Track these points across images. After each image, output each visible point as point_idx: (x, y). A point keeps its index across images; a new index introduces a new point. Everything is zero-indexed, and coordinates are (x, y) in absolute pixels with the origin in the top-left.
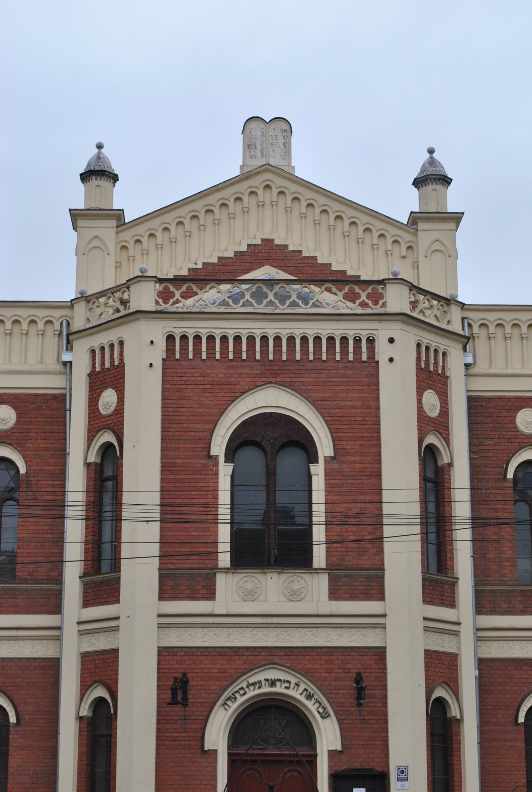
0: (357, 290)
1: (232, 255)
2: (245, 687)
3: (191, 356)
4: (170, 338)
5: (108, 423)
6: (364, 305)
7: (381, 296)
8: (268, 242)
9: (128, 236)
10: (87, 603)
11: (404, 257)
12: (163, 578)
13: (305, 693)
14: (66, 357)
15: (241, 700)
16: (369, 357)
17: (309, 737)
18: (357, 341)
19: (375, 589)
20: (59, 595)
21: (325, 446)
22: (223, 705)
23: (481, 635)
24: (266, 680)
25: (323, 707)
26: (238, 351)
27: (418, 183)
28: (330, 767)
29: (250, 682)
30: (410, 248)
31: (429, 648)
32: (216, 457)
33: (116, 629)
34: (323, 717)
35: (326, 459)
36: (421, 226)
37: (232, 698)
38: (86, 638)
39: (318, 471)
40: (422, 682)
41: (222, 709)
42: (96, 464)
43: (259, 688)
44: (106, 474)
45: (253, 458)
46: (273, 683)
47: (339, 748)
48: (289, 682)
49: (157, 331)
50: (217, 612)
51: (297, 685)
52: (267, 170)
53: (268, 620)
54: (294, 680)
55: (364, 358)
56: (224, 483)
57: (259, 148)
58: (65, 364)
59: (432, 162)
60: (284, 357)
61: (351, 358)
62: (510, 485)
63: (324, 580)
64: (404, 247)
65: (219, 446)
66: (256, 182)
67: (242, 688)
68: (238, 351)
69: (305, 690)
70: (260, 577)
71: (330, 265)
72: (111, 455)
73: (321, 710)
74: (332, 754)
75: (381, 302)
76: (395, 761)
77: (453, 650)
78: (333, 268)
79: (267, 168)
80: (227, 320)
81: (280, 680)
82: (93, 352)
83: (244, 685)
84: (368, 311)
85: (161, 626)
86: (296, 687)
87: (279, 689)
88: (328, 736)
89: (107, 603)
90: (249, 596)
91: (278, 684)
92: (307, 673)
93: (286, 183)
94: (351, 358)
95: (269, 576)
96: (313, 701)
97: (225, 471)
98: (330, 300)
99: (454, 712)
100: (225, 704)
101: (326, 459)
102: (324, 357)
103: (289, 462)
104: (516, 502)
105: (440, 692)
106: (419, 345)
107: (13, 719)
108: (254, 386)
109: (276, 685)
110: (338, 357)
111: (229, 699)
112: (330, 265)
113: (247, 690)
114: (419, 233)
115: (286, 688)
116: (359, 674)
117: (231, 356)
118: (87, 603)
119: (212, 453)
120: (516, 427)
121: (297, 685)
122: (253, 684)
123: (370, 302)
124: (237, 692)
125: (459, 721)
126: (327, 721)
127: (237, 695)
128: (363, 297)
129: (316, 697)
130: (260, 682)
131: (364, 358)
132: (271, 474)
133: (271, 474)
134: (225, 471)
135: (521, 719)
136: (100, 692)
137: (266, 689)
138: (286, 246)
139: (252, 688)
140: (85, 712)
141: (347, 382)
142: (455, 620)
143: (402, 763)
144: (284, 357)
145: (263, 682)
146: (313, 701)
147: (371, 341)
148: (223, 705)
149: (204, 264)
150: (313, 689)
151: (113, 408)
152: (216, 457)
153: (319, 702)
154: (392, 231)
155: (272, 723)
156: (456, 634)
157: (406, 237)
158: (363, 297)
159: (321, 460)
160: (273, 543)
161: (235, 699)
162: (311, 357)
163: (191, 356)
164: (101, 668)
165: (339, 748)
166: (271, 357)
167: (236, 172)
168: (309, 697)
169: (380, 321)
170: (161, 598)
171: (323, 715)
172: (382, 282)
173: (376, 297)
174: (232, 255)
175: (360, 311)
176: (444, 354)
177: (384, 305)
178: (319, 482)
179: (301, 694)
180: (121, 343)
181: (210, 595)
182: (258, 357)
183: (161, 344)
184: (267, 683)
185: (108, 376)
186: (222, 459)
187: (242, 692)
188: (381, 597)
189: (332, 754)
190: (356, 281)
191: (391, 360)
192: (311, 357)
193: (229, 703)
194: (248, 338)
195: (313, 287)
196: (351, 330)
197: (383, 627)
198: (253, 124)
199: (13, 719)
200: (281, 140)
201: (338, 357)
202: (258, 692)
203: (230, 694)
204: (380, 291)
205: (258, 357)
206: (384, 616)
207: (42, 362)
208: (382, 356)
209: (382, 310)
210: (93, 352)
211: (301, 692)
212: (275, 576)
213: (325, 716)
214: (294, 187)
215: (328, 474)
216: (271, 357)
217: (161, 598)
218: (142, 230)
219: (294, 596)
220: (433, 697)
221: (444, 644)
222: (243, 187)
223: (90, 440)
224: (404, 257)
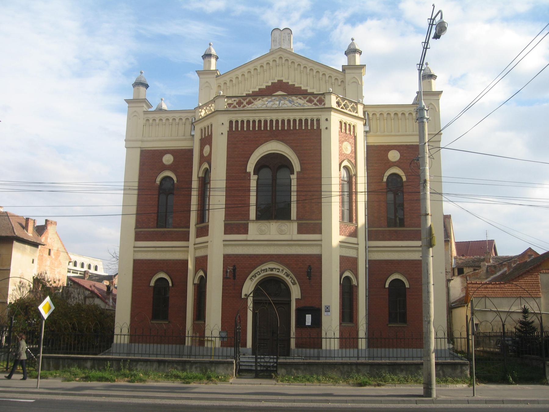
0: (313, 98)
1: (265, 87)
3: (239, 129)
4: (231, 122)
5: (206, 159)
6: (315, 104)
7: (323, 101)
8: (280, 81)
9: (221, 81)
10: (198, 236)
11: (340, 86)
12: (226, 226)
14: (192, 133)
15: (258, 277)
16: (317, 127)
17: (256, 292)
18: (312, 121)
19: (317, 228)
20: (188, 233)
21: (297, 167)
23: (368, 249)
26: (260, 126)
27: (346, 53)
28: (296, 306)
30: (342, 81)
31: (342, 255)
32: (250, 173)
33: (207, 247)
34: (293, 284)
35: (298, 173)
36: (347, 71)
37: (255, 276)
38: (197, 251)
39: (294, 177)
40: (338, 269)
41: (250, 281)
42: (202, 177)
44: (205, 182)
45: (267, 173)
46: (272, 270)
47: (300, 298)
49: (225, 119)
50: (248, 239)
51: (283, 270)
52: (281, 51)
53: (271, 242)
54: (281, 269)
55: (315, 128)
56: (253, 184)
57: (278, 41)
58: (191, 135)
59: (352, 44)
60: (280, 129)
61: (309, 128)
62: (385, 184)
63: (295, 226)
64: (340, 81)
65: (250, 168)
66: (276, 56)
68: (260, 126)
70: (268, 224)
71: (307, 90)
72: (207, 172)
74: (297, 300)
75: (323, 103)
76: (324, 303)
77: (355, 256)
78: (302, 89)
79: (281, 49)
80: (255, 113)
82: (202, 130)
83: (260, 270)
84: (317, 107)
85: (224, 245)
87: (274, 272)
88: (296, 292)
89: (205, 236)
90: (262, 233)
91: (274, 270)
92: (288, 266)
93: (289, 56)
94: (309, 128)
95: (271, 223)
97: (254, 179)
98: (300, 102)
99: (354, 282)
100: (251, 278)
101: (298, 173)
102: (297, 128)
103: (282, 174)
104: (387, 192)
105: (347, 274)
106: (341, 122)
107: (170, 285)
108: (266, 141)
110: (303, 128)
111: (253, 276)
112: (294, 85)
114: (346, 75)
116: (310, 266)
117: (257, 129)
118: (198, 236)
119: (248, 171)
120: (388, 158)
121: (283, 270)
123: (318, 104)
125: (357, 287)
126: (295, 286)
128: (315, 101)
130: (266, 269)
131: (315, 128)
132: (274, 179)
133: (274, 179)
134: (254, 179)
135: (387, 286)
136: (201, 273)
138: (288, 83)
140: (196, 282)
141: (308, 139)
142: (356, 242)
143: (328, 304)
144: (280, 129)
147: (318, 121)
149: (253, 92)
150: (289, 272)
151: (208, 153)
152: (250, 173)
154: (334, 75)
155: (272, 287)
156: (357, 249)
157: (340, 77)
158: (315, 101)
159: (295, 173)
160: (274, 209)
162: (292, 128)
163: (239, 129)
164: (202, 263)
165: (300, 298)
166: (274, 129)
167: (268, 52)
168: (288, 276)
169: (322, 111)
170: (225, 233)
172: (323, 94)
173: (321, 101)
174: (265, 87)
175: (314, 107)
176: (354, 126)
177: (324, 105)
178: (294, 182)
180: (212, 125)
181: (246, 232)
182: (268, 129)
183: (227, 125)
185: (206, 140)
186: (252, 173)
188: (320, 232)
189: (297, 300)
190: (312, 94)
191: (326, 128)
192: (292, 128)
193: (253, 278)
194: (264, 121)
195: (294, 98)
196: (309, 115)
197: (321, 245)
198: (275, 32)
199: (170, 285)
200: (287, 38)
201: (303, 128)
202: (265, 273)
204: (323, 98)
205: (268, 129)
206: (321, 240)
207: (184, 136)
208: (323, 127)
209: (323, 107)
210: (202, 130)
212: (274, 224)
213: (294, 284)
214: (292, 57)
215: (298, 179)
216: (274, 129)
217: (225, 233)
218: (227, 79)
219: (281, 232)
220: (344, 276)
221: (351, 253)
222: (270, 58)
223: (200, 167)
224: (340, 86)
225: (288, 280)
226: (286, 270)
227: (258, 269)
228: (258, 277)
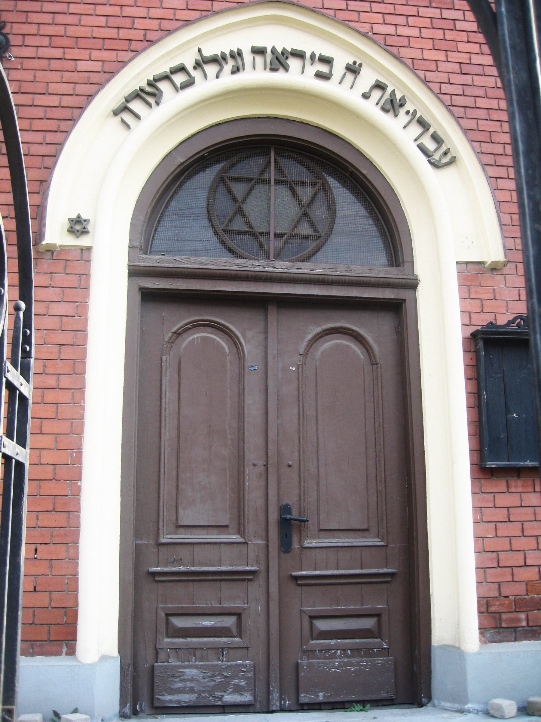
2: (190, 67)
13: (376, 94)
22: (116, 113)
24: (259, 51)
25: (435, 138)
29: (207, 53)
34: (435, 165)
37: (149, 93)
43: (236, 70)
48: (327, 61)
51: (353, 70)
54: (341, 60)
67: (182, 69)
69: (379, 86)
73: (431, 146)
81: (299, 55)
86: (350, 77)
87: (297, 76)
91: (294, 63)
96: (403, 118)
100: (125, 109)
109: (286, 69)
111: (138, 95)
113: (197, 75)
115: (319, 75)
121: (353, 70)
122: (214, 60)
124: (166, 77)
127: (163, 86)
129: (409, 106)
130: (237, 55)
137: (256, 75)
139: (211, 69)
145: (248, 57)
146: (403, 118)
148: (116, 113)
153: (423, 124)
161: (157, 95)
168: (393, 106)
171: (437, 156)
179: (366, 96)
184: (259, 59)
187: (179, 79)
193: (136, 106)
202: (228, 81)
203: (143, 84)
211: (367, 90)
213: (441, 159)
225: (391, 146)
226: (381, 66)
227: (176, 49)
228: (173, 101)
